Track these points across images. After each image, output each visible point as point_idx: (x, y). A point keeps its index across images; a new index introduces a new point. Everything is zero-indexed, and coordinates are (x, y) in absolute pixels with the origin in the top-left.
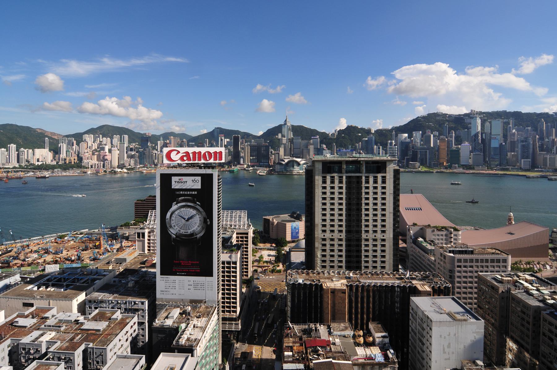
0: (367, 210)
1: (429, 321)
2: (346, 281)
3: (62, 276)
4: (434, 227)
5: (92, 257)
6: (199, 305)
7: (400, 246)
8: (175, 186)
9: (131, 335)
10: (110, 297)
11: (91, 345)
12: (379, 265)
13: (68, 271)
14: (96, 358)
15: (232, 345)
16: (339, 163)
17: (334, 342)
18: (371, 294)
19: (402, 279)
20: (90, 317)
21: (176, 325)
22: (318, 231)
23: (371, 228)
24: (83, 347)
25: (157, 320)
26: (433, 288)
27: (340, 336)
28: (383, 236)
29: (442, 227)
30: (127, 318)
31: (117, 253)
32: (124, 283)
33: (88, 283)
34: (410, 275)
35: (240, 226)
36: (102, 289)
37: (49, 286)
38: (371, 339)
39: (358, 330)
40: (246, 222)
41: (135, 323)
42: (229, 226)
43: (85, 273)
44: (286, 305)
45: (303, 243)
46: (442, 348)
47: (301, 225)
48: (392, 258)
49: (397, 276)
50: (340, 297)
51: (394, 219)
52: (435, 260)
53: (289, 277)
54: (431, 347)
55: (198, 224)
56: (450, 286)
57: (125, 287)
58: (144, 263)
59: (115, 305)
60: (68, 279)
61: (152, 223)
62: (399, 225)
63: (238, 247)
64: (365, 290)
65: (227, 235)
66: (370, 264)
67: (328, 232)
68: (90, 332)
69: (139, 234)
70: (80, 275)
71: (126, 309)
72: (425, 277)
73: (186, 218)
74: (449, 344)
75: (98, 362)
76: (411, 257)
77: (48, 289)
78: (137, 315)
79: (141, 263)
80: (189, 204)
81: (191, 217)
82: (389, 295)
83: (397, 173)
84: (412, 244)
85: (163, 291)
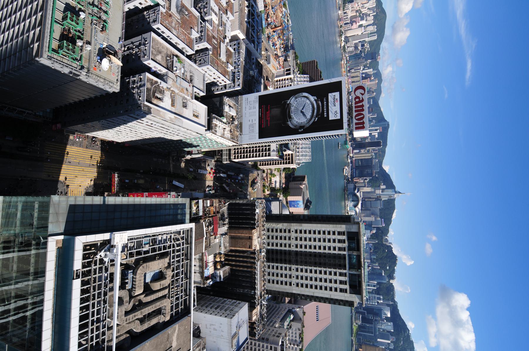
0: (316, 272)
1: (231, 316)
2: (258, 249)
3: (256, 16)
4: (302, 331)
5: (270, 35)
6: (239, 130)
7: (286, 298)
8: (331, 96)
9: (218, 81)
10: (242, 59)
11: (211, 53)
12: (271, 278)
13: (259, 20)
14: (203, 59)
15: (213, 157)
16: (358, 249)
17: (217, 238)
18: (249, 270)
19: (261, 297)
20: (229, 47)
21: (225, 115)
22: (296, 226)
23: (300, 274)
24: (209, 47)
25: (228, 99)
26: (254, 323)
27: (220, 242)
28: (294, 284)
29: (303, 338)
30: (229, 76)
31: (274, 54)
32: (252, 67)
33: (251, 38)
34: (263, 304)
35: (298, 156)
37: (248, 8)
38: (219, 267)
39: (225, 257)
40: (302, 161)
41: (225, 82)
42: (298, 146)
43: (259, 34)
44: (240, 198)
45: (286, 212)
46: (214, 324)
47: (300, 210)
48: (277, 290)
49: (263, 293)
50: (247, 244)
51: (309, 295)
52: (276, 327)
53: (260, 201)
54: (213, 315)
55: (298, 121)
56: (257, 338)
57: (249, 69)
58: (267, 79)
59: (237, 64)
60: (254, 21)
61: (299, 79)
62: (304, 299)
63: (281, 157)
64: (252, 265)
65: (291, 146)
66: (271, 270)
67: (296, 235)
68: (219, 49)
69: (289, 70)
70: (257, 30)
71: (234, 73)
72: (263, 317)
73: (304, 111)
74: (216, 330)
75: (200, 60)
76: (278, 306)
77: (246, 8)
78: (230, 83)
79: (267, 77)
80: (315, 111)
81: (304, 115)
82: (249, 285)
83: (350, 304)
84: (288, 309)
85: (247, 100)
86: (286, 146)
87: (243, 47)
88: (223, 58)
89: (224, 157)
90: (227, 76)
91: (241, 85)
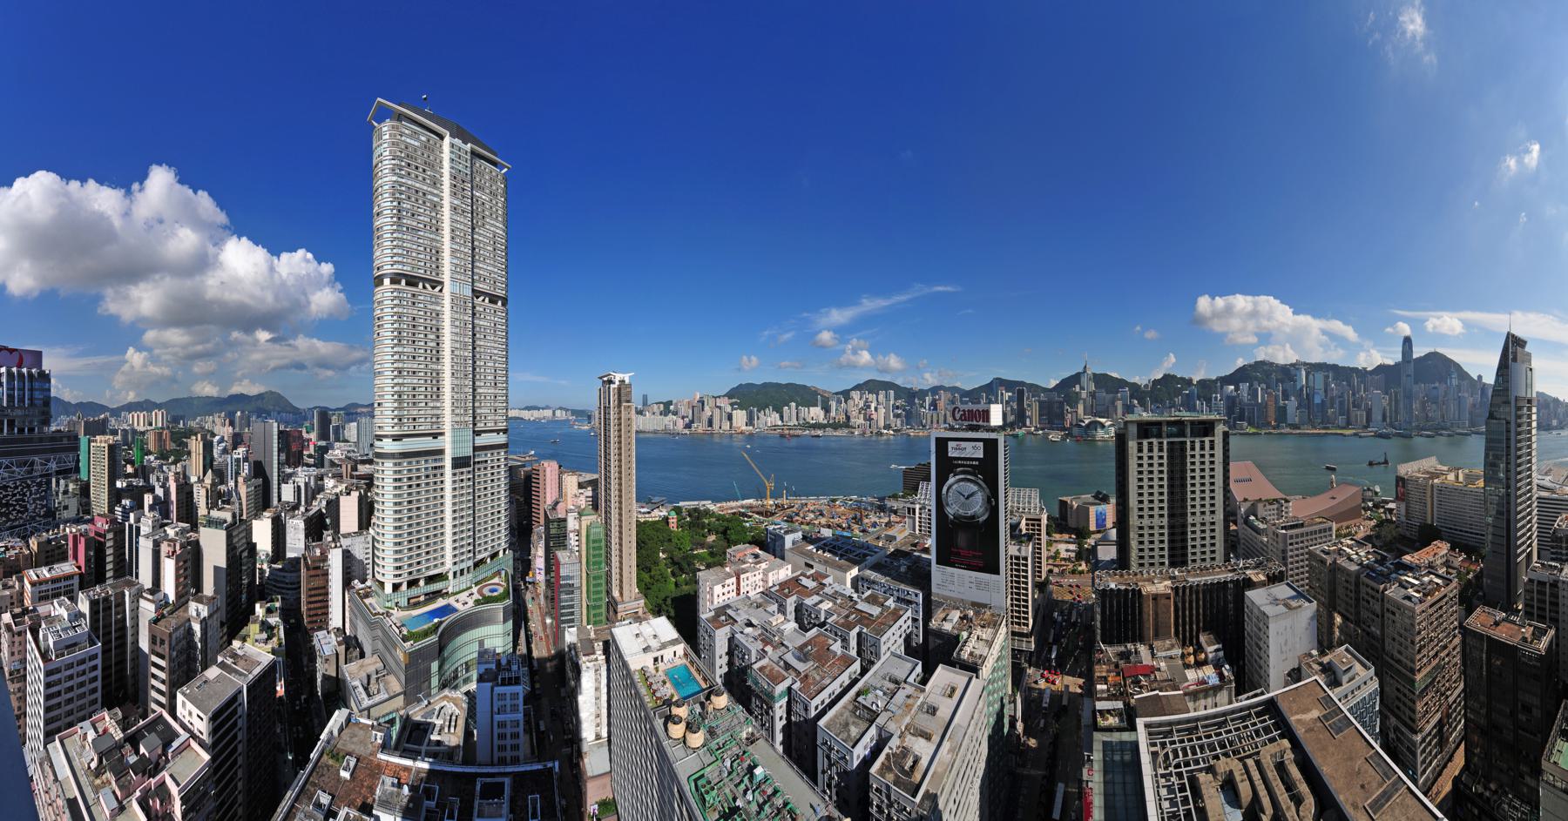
10: (882, 579)
36: (875, 568)
86: (1014, 527)
87: (868, 573)
88: (875, 611)
89: (1024, 647)
90: (901, 613)
91: (917, 591)
